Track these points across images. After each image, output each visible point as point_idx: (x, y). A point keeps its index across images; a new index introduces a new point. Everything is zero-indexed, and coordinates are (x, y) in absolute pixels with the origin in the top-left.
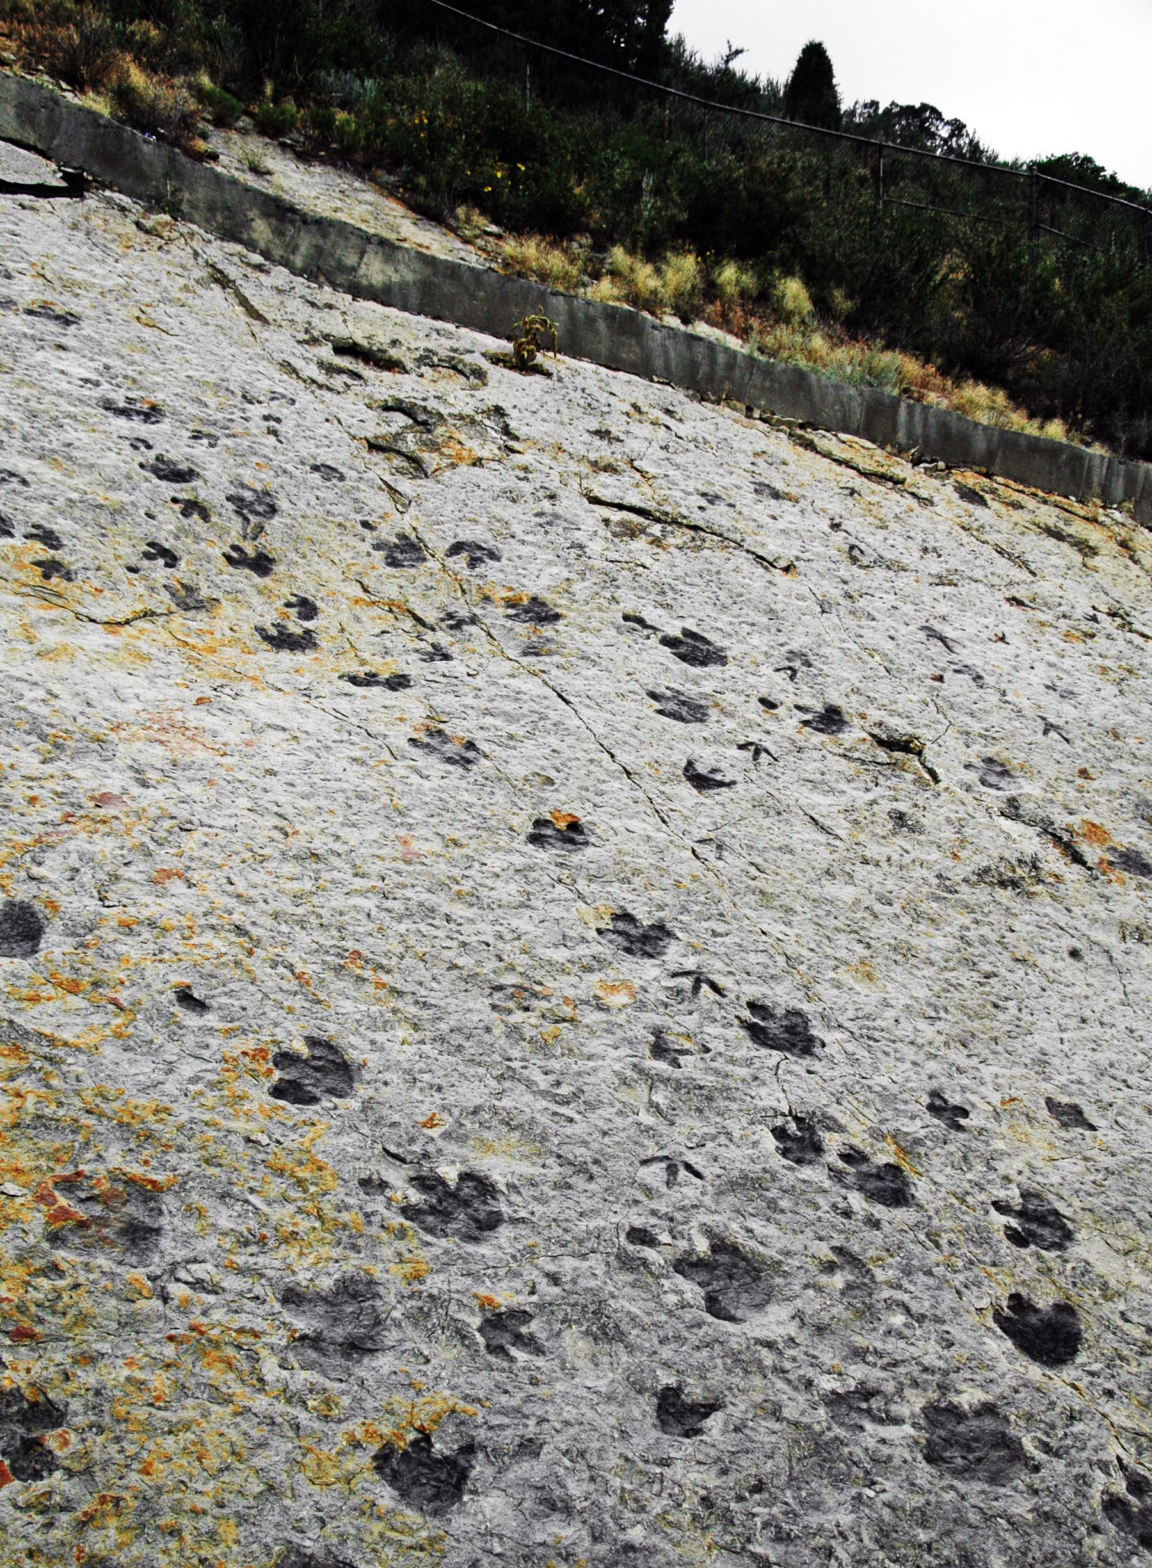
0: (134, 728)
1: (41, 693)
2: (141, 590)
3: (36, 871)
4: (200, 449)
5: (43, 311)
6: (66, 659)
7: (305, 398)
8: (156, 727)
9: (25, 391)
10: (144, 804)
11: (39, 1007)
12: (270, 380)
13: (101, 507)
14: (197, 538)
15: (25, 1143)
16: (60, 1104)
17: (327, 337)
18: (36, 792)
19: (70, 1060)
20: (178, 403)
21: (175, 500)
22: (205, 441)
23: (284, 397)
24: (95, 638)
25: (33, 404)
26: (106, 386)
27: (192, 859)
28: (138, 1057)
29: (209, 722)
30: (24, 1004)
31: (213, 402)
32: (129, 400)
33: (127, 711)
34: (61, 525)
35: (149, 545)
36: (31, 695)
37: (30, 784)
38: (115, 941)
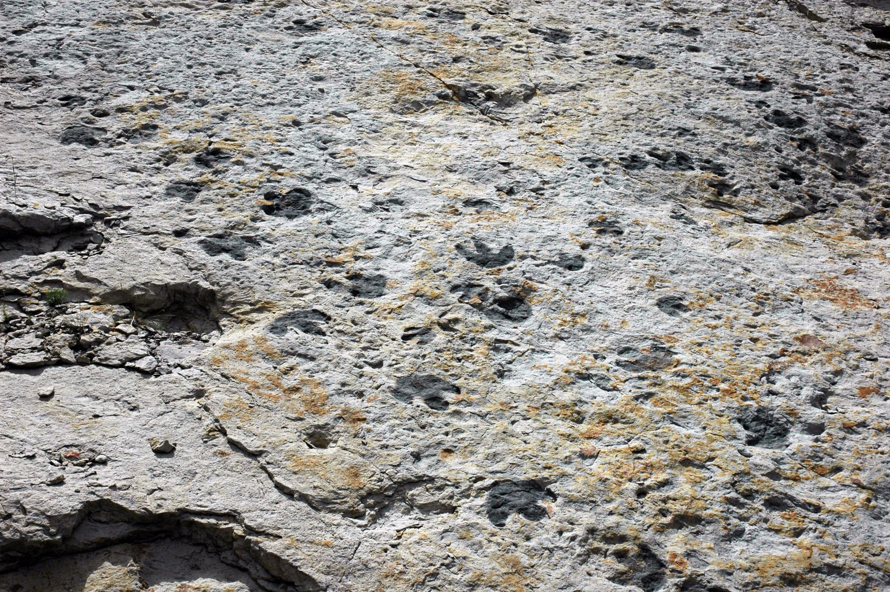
0: (809, 292)
1: (740, 270)
2: (782, 199)
3: (775, 388)
4: (802, 104)
5: (677, 28)
6: (747, 246)
7: (863, 66)
8: (823, 290)
9: (681, 78)
10: (834, 342)
11: (802, 485)
12: (835, 57)
13: (745, 146)
14: (813, 163)
15: (818, 583)
16: (837, 556)
17: (866, 25)
18: (756, 335)
19: (837, 523)
20: (778, 77)
21: (792, 139)
22: (804, 100)
23: (850, 66)
24: (761, 233)
25: (687, 86)
26: (729, 70)
27: (881, 380)
28: (885, 524)
29: (857, 285)
30: (790, 482)
31: (803, 74)
32: (746, 78)
33: (799, 279)
34: (722, 159)
35: (782, 170)
36: (735, 270)
37: (752, 330)
38: (844, 438)
